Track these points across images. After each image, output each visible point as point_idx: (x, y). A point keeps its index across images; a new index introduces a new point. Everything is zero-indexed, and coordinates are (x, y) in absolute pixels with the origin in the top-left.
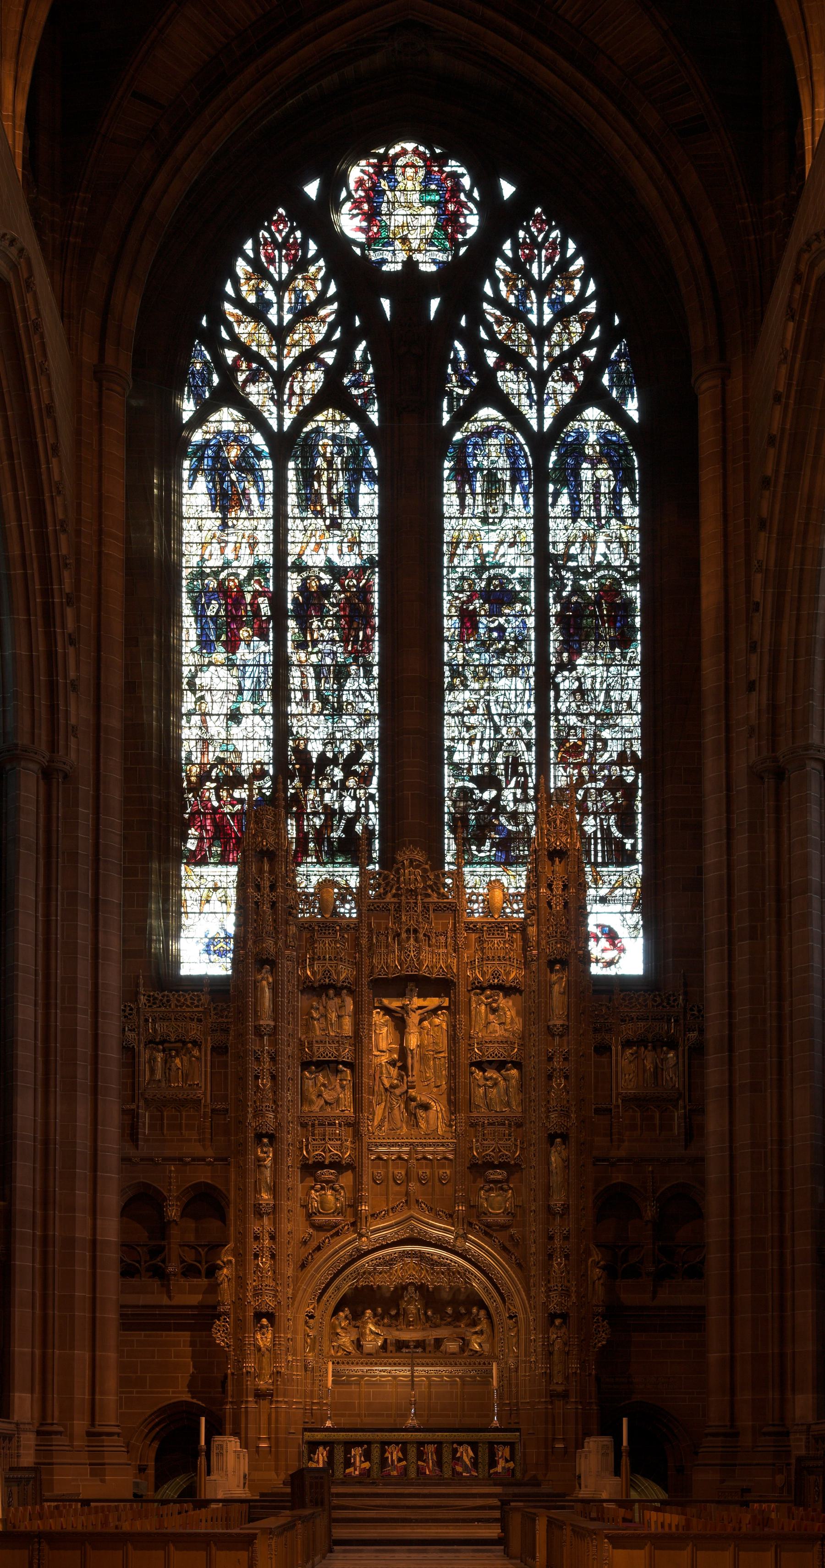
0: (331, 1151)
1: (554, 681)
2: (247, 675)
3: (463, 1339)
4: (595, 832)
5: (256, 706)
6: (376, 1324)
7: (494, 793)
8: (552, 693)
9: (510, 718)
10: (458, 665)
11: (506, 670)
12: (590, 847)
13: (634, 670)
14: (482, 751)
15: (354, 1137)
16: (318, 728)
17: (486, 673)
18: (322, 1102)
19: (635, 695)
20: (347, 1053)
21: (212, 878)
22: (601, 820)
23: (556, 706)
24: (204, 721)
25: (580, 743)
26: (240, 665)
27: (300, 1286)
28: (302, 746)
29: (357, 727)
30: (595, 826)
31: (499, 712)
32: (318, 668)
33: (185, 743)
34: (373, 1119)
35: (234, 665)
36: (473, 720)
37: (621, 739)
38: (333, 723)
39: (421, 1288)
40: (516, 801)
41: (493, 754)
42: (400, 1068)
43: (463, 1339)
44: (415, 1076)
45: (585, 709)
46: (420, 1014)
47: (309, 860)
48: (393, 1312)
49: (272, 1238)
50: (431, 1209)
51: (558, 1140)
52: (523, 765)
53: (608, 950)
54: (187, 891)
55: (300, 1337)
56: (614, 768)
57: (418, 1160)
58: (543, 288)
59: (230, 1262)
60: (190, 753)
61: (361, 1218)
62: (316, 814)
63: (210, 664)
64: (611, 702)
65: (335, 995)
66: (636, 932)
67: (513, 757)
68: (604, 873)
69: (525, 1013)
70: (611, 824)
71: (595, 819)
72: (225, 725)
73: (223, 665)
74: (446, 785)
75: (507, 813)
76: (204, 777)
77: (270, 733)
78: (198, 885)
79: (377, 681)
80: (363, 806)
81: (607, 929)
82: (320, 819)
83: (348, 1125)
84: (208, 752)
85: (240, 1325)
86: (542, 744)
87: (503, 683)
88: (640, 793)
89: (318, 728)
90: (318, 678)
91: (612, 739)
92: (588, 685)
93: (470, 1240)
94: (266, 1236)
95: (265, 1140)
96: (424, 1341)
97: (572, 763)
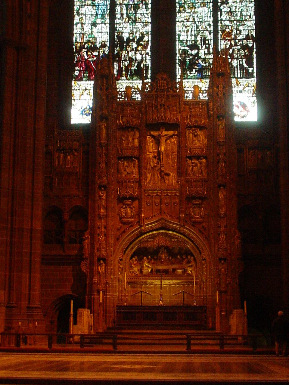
0: (129, 192)
1: (220, 8)
2: (99, 9)
3: (184, 269)
4: (237, 66)
5: (103, 20)
6: (149, 263)
7: (196, 51)
8: (219, 13)
9: (203, 23)
10: (182, 3)
11: (201, 4)
12: (235, 71)
13: (252, 4)
14: (191, 35)
15: (139, 187)
16: (127, 28)
17: (193, 6)
18: (126, 173)
19: (253, 13)
20: (136, 153)
21: (85, 86)
22: (239, 61)
23: (221, 18)
24: (82, 26)
25: (231, 32)
26: (97, 5)
27: (116, 247)
28: (121, 35)
29: (142, 27)
30: (237, 63)
31: (198, 20)
32: (127, 6)
33: (75, 35)
34: (147, 180)
35: (94, 5)
36: (188, 24)
37: (247, 30)
38: (133, 26)
39: (167, 248)
40: (205, 54)
41: (196, 36)
42: (158, 159)
43: (184, 269)
44: (164, 161)
45: (232, 19)
46: (166, 138)
47: (123, 78)
48: (156, 257)
49: (105, 227)
50: (170, 215)
51: (222, 187)
52: (208, 40)
53: (243, 111)
54: (74, 91)
55: (116, 268)
56: (244, 41)
57: (165, 196)
59: (88, 237)
60: (76, 38)
61: (141, 219)
62: (126, 60)
63: (85, 5)
64: (243, 16)
65: (131, 131)
66: (254, 104)
67: (204, 38)
68: (241, 82)
69: (208, 137)
70: (243, 62)
71: (237, 60)
72: (90, 28)
73: (90, 5)
74: (177, 49)
75: (201, 59)
76: (82, 47)
77: (108, 31)
78: (79, 88)
79: (150, 10)
80: (144, 57)
81: (242, 103)
82: (127, 62)
83: (136, 182)
84: (84, 38)
87: (200, 10)
88: (255, 50)
89: (127, 28)
90: (127, 9)
91: (243, 30)
92: (233, 10)
93: (186, 228)
94: (103, 227)
95: (103, 188)
96: (168, 270)
97: (228, 39)
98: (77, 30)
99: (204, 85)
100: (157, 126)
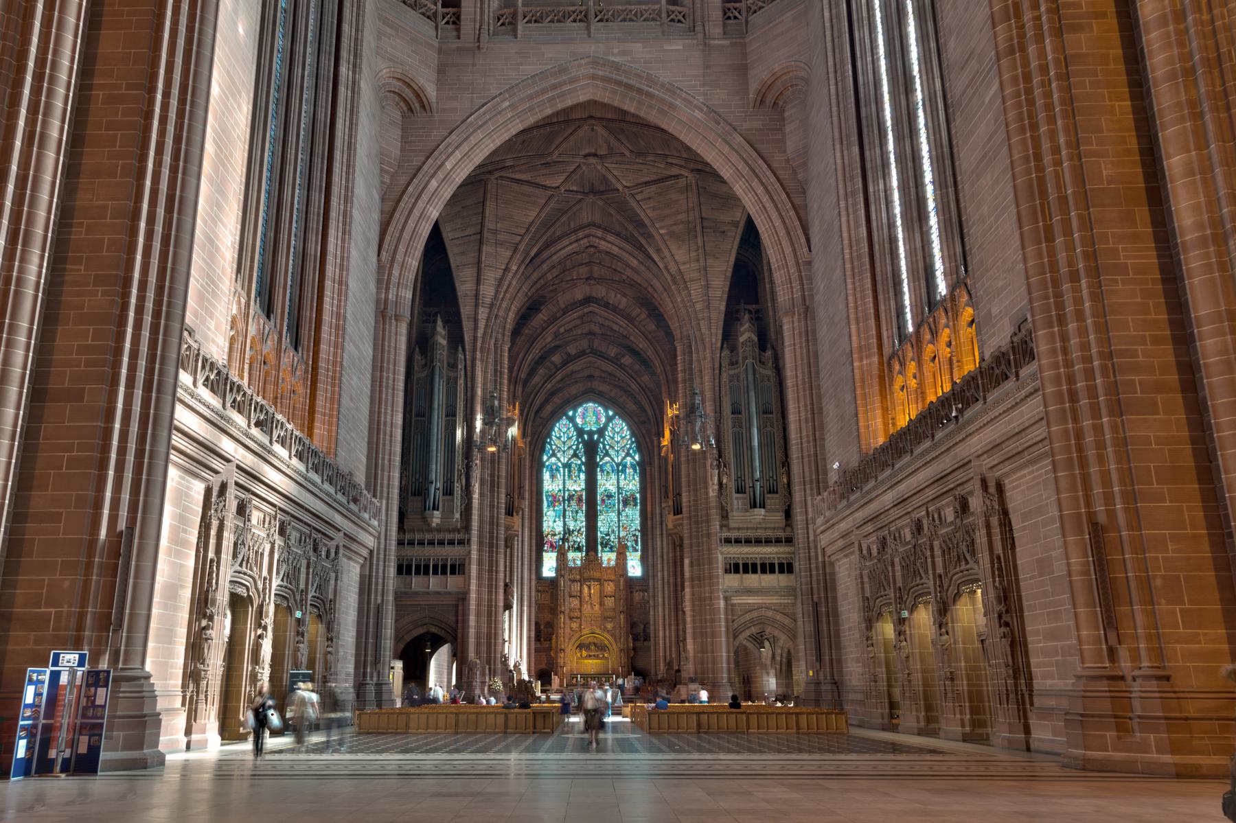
58: (618, 433)
85: (557, 652)
86: (619, 527)
98: (545, 524)
99: (613, 556)
100: (590, 579)
